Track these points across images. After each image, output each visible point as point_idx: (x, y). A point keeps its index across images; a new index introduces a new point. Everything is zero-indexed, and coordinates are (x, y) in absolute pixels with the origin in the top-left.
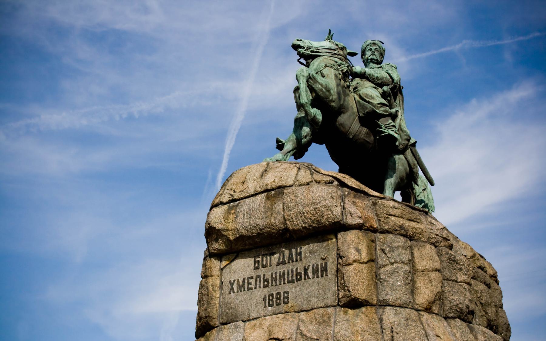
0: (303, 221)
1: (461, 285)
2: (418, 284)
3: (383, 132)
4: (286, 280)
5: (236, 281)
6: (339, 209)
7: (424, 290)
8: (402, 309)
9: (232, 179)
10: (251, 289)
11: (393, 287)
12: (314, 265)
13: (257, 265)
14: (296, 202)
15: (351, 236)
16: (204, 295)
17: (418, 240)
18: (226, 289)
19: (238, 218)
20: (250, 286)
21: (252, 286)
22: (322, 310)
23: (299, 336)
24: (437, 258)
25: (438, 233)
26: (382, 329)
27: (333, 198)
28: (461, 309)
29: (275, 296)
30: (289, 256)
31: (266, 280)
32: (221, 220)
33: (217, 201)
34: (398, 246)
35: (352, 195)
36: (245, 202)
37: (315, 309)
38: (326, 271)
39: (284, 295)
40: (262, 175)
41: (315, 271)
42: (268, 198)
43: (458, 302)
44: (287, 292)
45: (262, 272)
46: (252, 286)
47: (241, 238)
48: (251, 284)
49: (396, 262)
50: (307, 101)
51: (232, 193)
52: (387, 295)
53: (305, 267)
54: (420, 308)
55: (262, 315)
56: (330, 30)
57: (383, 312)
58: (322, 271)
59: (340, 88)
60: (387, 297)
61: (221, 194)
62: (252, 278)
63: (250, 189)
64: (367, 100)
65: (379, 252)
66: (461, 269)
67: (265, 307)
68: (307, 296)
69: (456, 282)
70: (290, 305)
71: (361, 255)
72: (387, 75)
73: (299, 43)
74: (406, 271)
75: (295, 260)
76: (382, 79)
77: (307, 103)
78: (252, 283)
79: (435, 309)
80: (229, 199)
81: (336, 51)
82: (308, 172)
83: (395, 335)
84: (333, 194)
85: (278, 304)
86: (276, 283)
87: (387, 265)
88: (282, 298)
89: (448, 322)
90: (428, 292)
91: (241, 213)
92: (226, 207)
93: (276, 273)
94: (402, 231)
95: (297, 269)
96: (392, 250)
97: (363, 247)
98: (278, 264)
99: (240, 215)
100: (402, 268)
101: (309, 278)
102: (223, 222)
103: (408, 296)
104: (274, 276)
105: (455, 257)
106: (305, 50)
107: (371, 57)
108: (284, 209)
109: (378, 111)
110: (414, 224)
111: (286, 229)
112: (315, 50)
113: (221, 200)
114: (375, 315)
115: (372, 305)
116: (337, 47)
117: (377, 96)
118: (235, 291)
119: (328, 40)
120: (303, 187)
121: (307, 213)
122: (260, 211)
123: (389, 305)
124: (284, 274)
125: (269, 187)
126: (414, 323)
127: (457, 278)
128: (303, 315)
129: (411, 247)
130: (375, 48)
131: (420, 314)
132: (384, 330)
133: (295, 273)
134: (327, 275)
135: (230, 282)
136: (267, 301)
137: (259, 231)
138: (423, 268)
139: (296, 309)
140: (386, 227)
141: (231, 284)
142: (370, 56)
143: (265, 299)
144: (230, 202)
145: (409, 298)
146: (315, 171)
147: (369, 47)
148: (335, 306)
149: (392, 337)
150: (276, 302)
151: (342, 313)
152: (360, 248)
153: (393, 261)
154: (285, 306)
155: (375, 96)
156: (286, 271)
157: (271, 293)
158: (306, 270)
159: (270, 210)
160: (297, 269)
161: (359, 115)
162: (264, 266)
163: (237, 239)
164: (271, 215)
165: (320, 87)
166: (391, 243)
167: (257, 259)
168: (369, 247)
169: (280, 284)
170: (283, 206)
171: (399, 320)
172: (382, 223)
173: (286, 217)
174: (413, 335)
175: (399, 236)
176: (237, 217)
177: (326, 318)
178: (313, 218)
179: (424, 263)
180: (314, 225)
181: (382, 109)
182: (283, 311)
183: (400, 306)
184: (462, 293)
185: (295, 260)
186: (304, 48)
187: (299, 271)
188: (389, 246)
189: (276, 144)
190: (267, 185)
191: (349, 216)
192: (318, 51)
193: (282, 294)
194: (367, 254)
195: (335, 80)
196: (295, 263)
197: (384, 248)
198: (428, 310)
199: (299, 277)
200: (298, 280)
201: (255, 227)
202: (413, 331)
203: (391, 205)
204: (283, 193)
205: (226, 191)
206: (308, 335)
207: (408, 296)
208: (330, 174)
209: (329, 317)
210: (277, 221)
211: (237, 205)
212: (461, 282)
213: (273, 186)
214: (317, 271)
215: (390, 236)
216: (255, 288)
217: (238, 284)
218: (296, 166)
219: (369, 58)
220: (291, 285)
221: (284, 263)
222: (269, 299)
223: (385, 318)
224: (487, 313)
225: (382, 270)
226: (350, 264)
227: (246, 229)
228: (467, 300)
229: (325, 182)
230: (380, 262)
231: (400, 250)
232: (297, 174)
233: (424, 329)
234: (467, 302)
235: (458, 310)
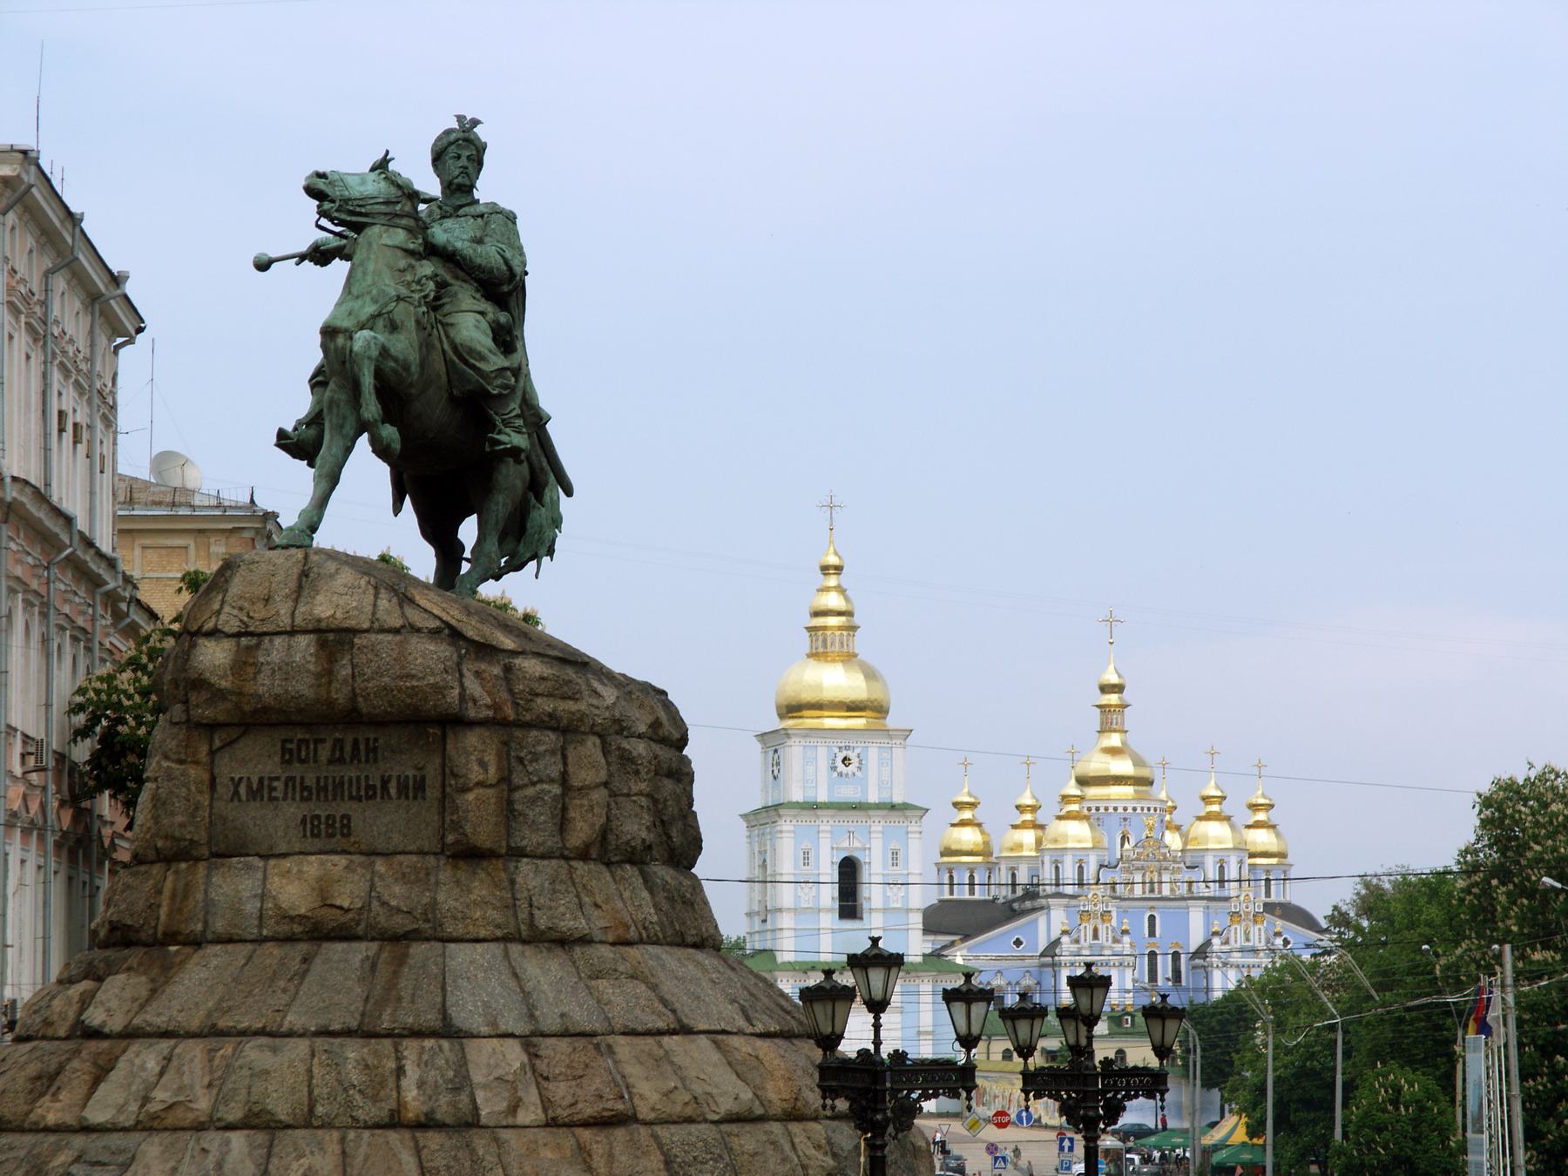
0: (389, 702)
1: (635, 802)
2: (571, 814)
3: (499, 442)
4: (346, 793)
5: (245, 781)
6: (457, 691)
7: (579, 824)
8: (546, 862)
9: (237, 580)
10: (276, 799)
11: (534, 826)
12: (399, 776)
13: (287, 757)
14: (379, 667)
15: (472, 739)
16: (178, 797)
17: (576, 731)
18: (224, 790)
19: (262, 675)
20: (274, 794)
21: (278, 794)
22: (414, 858)
23: (375, 904)
24: (603, 761)
25: (607, 714)
26: (515, 899)
27: (447, 672)
28: (634, 848)
29: (323, 819)
30: (353, 750)
31: (304, 788)
32: (225, 672)
33: (209, 626)
34: (546, 751)
35: (473, 656)
36: (271, 641)
37: (400, 853)
38: (424, 791)
39: (341, 821)
40: (300, 587)
41: (403, 789)
42: (322, 645)
43: (629, 837)
44: (346, 817)
45: (297, 770)
46: (278, 794)
47: (266, 709)
48: (275, 789)
49: (541, 781)
50: (376, 416)
51: (245, 619)
52: (524, 838)
53: (383, 777)
54: (572, 855)
55: (297, 850)
56: (537, 577)
57: (517, 868)
58: (414, 788)
59: (424, 350)
60: (524, 843)
61: (219, 612)
62: (277, 779)
63: (284, 618)
64: (472, 361)
65: (513, 762)
66: (637, 772)
67: (305, 836)
68: (384, 829)
69: (628, 795)
70: (352, 839)
71: (486, 771)
72: (502, 261)
73: (321, 184)
74: (556, 795)
75: (363, 759)
76: (491, 271)
77: (376, 421)
78: (279, 789)
79: (594, 853)
80: (238, 629)
81: (400, 205)
82: (395, 600)
83: (536, 912)
84: (448, 663)
85: (332, 836)
86: (326, 796)
87: (525, 786)
88: (338, 825)
89: (611, 872)
90: (586, 827)
91: (267, 667)
92: (233, 641)
93: (326, 778)
94: (553, 723)
95: (367, 777)
96: (536, 758)
97: (491, 758)
98: (330, 762)
99: (266, 670)
100: (550, 792)
101: (390, 797)
102: (231, 678)
103: (555, 840)
104: (322, 784)
105: (630, 753)
106: (336, 211)
107: (460, 180)
108: (353, 676)
109: (489, 388)
110: (571, 706)
111: (355, 709)
112: (358, 209)
113: (220, 627)
114: (503, 875)
115: (497, 856)
116: (400, 193)
117: (490, 351)
118: (244, 797)
119: (381, 173)
120: (390, 637)
121: (399, 692)
122: (308, 671)
123: (526, 856)
124: (342, 783)
125: (323, 625)
126: (562, 888)
127: (630, 788)
128: (380, 865)
129: (563, 749)
130: (467, 153)
131: (571, 866)
132: (518, 903)
133: (363, 783)
134: (424, 798)
135: (232, 779)
136: (309, 826)
137: (303, 706)
138: (581, 784)
139: (363, 847)
140: (528, 717)
141: (233, 784)
142: (457, 177)
143: (304, 821)
144: (238, 635)
145: (557, 843)
146: (407, 597)
147: (453, 147)
148: (435, 854)
149: (532, 915)
150: (327, 832)
151: (449, 867)
152: (486, 759)
153: (535, 779)
154: (344, 840)
155: (486, 351)
156: (346, 778)
157: (317, 813)
158: (385, 783)
159: (328, 673)
160: (367, 777)
161: (452, 392)
162: (302, 761)
163: (255, 711)
164: (330, 683)
165: (392, 364)
166: (534, 746)
167: (289, 746)
168: (499, 755)
169: (335, 799)
170: (353, 669)
171: (542, 886)
172: (521, 709)
173: (358, 691)
174: (562, 909)
175: (546, 732)
176: (259, 672)
177: (422, 875)
178: (408, 701)
179: (583, 774)
180: (408, 712)
181: (499, 382)
182: (339, 849)
183: (543, 857)
184: (636, 816)
185: (363, 759)
186: (333, 201)
187: (371, 783)
188: (531, 752)
189: (274, 440)
190: (319, 621)
191: (470, 704)
192: (363, 210)
193: (338, 819)
194: (497, 770)
195: (417, 334)
196: (363, 765)
197: (522, 755)
198: (584, 855)
199: (371, 793)
200: (374, 796)
201: (297, 698)
202: (563, 902)
203: (537, 675)
204: (352, 644)
205: (227, 609)
206: (394, 903)
207: (555, 840)
208: (435, 611)
209: (428, 874)
210: (340, 696)
211: (258, 646)
212: (635, 795)
213: (333, 626)
214: (407, 787)
215: (534, 733)
216: (285, 799)
217: (249, 786)
218: (369, 582)
219: (456, 181)
220: (355, 805)
221: (341, 761)
222: (312, 824)
223: (519, 880)
224: (670, 837)
225: (517, 795)
226: (469, 790)
227: (277, 696)
228: (643, 828)
229: (429, 632)
230: (517, 779)
231: (547, 758)
232: (375, 605)
233: (578, 896)
234: (644, 834)
235: (629, 849)
